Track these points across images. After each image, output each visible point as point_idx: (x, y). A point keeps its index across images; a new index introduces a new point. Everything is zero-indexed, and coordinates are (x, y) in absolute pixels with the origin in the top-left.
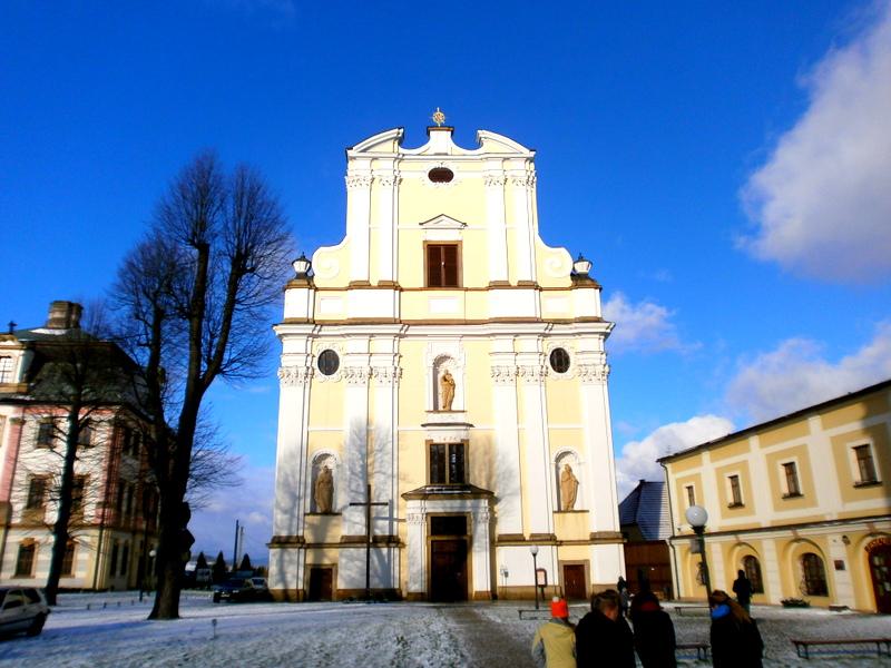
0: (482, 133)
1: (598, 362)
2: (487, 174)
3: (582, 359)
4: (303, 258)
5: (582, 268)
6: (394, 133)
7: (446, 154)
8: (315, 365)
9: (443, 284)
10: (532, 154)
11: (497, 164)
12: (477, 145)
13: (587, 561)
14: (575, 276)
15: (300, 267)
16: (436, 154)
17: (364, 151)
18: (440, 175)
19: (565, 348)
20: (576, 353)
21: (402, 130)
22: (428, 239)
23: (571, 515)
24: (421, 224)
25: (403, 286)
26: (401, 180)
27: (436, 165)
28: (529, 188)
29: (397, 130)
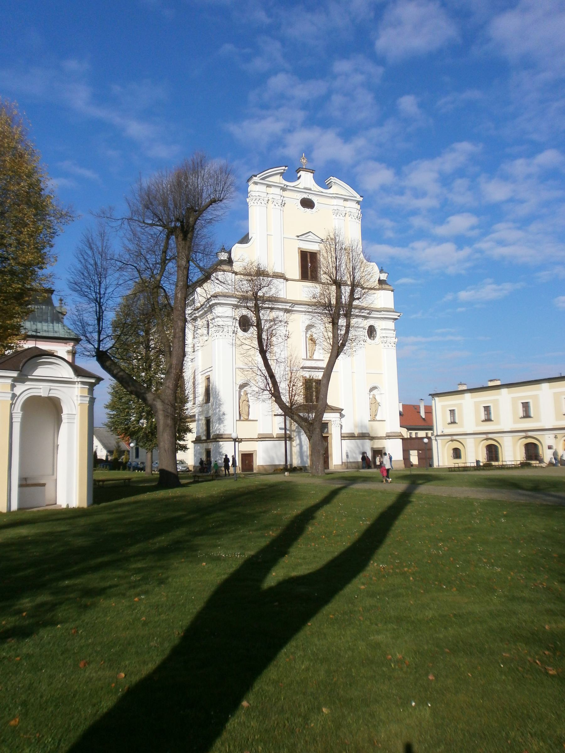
0: (333, 179)
1: (392, 335)
2: (336, 208)
3: (384, 333)
4: (223, 250)
5: (384, 277)
6: (281, 169)
7: (310, 190)
8: (237, 325)
9: (309, 278)
10: (361, 199)
11: (341, 202)
12: (328, 187)
13: (384, 448)
14: (381, 282)
15: (223, 256)
16: (305, 189)
17: (262, 179)
18: (307, 204)
19: (375, 326)
20: (382, 329)
21: (287, 168)
22: (300, 247)
23: (377, 422)
24: (298, 236)
25: (287, 276)
26: (285, 203)
27: (305, 196)
28: (358, 221)
29: (284, 168)
